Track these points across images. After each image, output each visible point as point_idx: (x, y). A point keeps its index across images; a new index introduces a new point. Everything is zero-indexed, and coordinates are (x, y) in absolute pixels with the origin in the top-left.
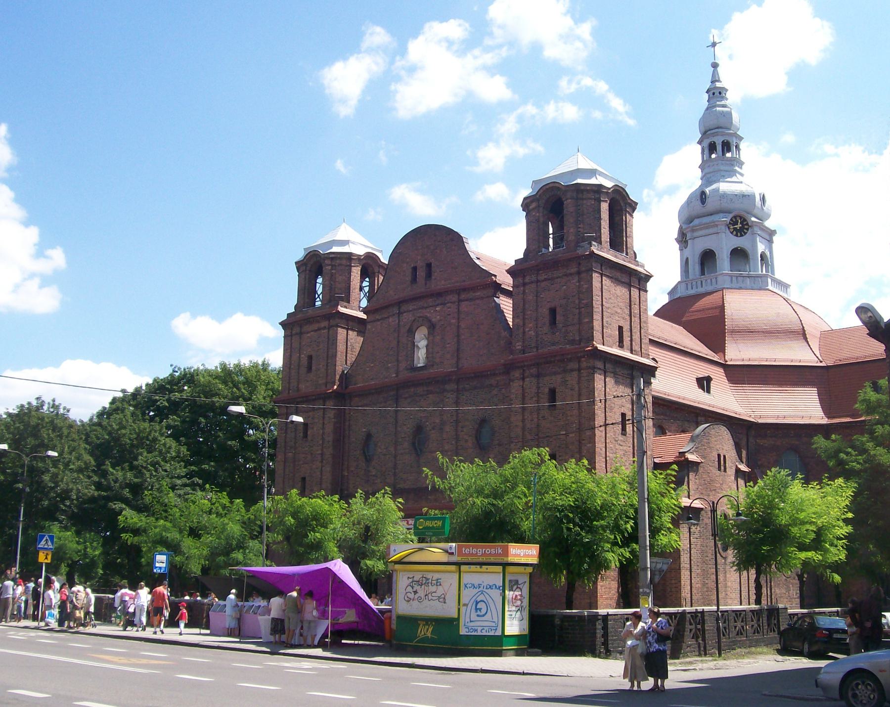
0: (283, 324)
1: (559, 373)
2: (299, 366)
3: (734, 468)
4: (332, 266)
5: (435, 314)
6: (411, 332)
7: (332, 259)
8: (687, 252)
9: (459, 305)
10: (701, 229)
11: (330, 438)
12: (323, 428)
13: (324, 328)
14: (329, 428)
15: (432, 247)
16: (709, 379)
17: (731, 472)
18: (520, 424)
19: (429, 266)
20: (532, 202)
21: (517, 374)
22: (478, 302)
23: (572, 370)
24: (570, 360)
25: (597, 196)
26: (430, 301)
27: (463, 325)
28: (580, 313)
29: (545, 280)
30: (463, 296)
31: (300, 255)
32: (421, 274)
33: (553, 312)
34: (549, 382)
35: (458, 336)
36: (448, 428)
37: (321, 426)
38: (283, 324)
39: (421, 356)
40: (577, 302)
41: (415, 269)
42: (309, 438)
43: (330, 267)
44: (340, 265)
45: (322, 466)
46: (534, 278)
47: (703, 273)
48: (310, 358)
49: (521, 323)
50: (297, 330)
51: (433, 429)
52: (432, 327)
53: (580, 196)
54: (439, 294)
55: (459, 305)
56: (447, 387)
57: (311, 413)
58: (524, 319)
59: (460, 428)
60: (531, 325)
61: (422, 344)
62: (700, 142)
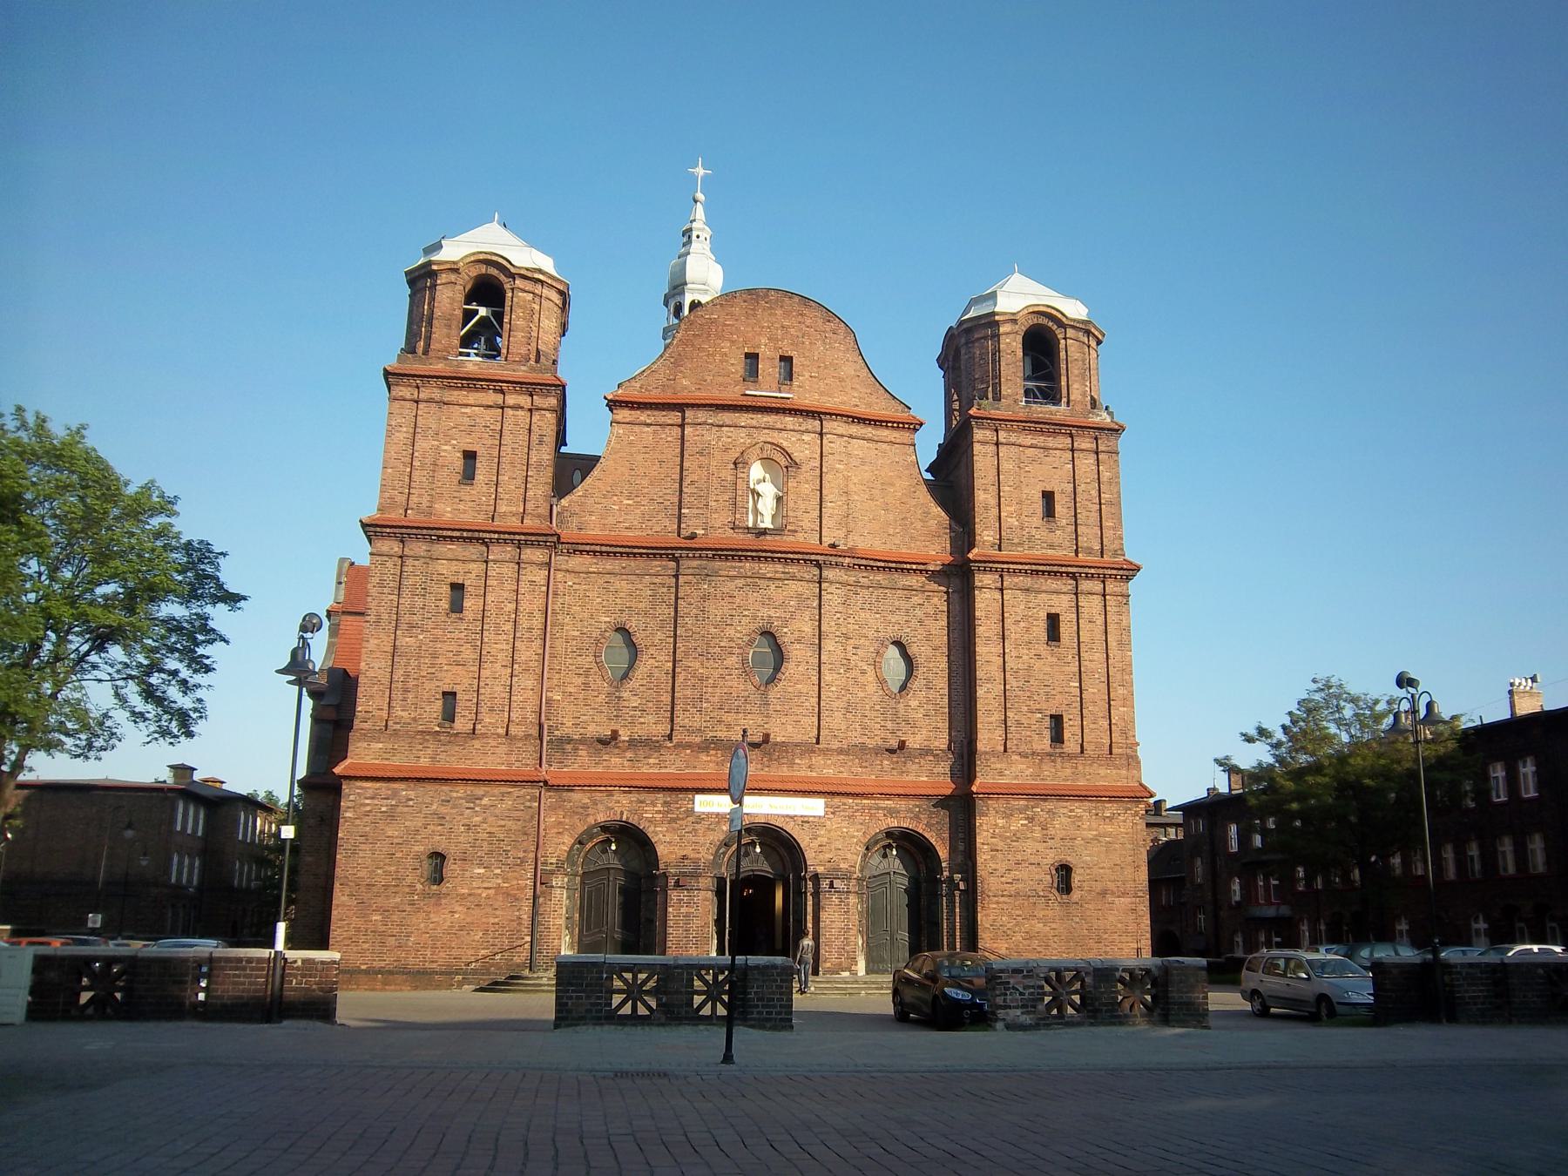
5: (799, 440)
19: (787, 360)
22: (884, 446)
32: (769, 369)
33: (1048, 497)
41: (752, 358)
51: (799, 641)
57: (472, 566)
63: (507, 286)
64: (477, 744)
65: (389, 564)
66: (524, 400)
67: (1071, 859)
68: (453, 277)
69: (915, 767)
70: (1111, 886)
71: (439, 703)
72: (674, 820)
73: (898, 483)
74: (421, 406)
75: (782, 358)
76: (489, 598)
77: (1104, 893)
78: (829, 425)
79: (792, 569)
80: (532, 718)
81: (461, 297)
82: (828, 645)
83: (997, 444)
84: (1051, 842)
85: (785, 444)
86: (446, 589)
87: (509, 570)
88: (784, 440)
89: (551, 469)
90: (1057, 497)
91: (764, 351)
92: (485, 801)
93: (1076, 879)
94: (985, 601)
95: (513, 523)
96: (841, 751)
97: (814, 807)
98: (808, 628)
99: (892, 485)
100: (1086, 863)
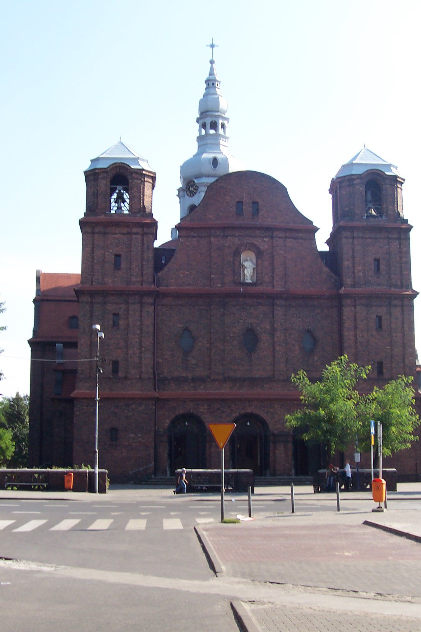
6: (237, 253)
12: (141, 320)
13: (137, 233)
18: (353, 338)
20: (357, 178)
22: (301, 241)
26: (258, 232)
29: (370, 238)
33: (377, 261)
45: (141, 353)
49: (351, 265)
52: (259, 254)
58: (354, 263)
60: (360, 268)
63: (129, 177)
64: (128, 382)
65: (87, 306)
66: (139, 230)
68: (105, 175)
71: (111, 366)
74: (96, 235)
75: (254, 203)
76: (130, 320)
78: (276, 233)
79: (260, 301)
80: (151, 371)
81: (109, 183)
82: (278, 334)
83: (353, 238)
85: (256, 243)
86: (111, 316)
87: (137, 307)
88: (255, 241)
89: (153, 261)
90: (381, 261)
91: (246, 200)
92: (133, 406)
94: (347, 312)
95: (138, 287)
98: (268, 327)
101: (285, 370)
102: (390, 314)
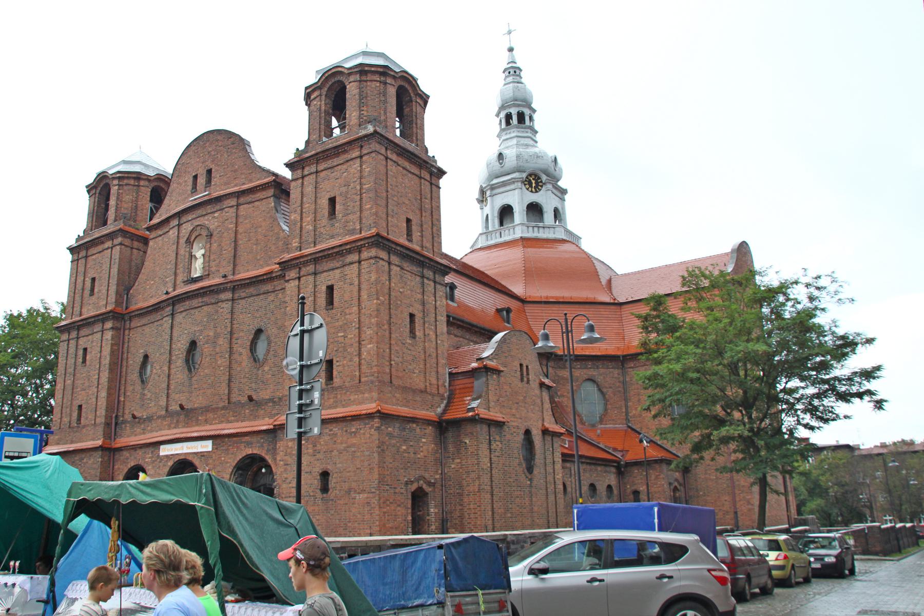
0: (72, 250)
1: (337, 268)
2: (83, 289)
3: (538, 381)
4: (119, 185)
5: (212, 221)
7: (119, 178)
8: (487, 210)
9: (237, 209)
10: (499, 187)
11: (106, 361)
14: (107, 350)
15: (213, 153)
16: (508, 311)
17: (535, 385)
19: (209, 172)
21: (293, 274)
23: (352, 263)
24: (350, 252)
25: (383, 79)
26: (209, 209)
27: (240, 230)
28: (361, 199)
30: (242, 200)
31: (90, 180)
32: (201, 181)
33: (332, 201)
34: (324, 280)
35: (236, 241)
36: (221, 341)
37: (99, 349)
38: (72, 250)
39: (197, 269)
40: (358, 187)
41: (195, 177)
42: (88, 363)
43: (117, 187)
44: (126, 185)
46: (313, 169)
47: (501, 224)
48: (93, 280)
50: (83, 253)
53: (364, 78)
54: (219, 199)
55: (237, 209)
56: (223, 296)
59: (233, 340)
61: (199, 253)
62: (497, 115)
67: (330, 468)
69: (262, 412)
70: (354, 485)
72: (154, 462)
73: (263, 224)
77: (349, 491)
84: (318, 456)
90: (337, 199)
93: (332, 482)
96: (224, 408)
97: (207, 446)
99: (261, 227)
100: (338, 466)
101: (226, 392)
102: (343, 277)
